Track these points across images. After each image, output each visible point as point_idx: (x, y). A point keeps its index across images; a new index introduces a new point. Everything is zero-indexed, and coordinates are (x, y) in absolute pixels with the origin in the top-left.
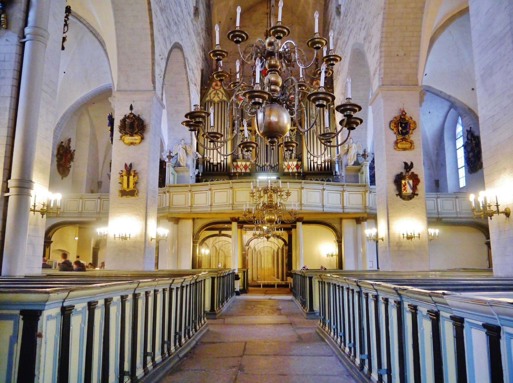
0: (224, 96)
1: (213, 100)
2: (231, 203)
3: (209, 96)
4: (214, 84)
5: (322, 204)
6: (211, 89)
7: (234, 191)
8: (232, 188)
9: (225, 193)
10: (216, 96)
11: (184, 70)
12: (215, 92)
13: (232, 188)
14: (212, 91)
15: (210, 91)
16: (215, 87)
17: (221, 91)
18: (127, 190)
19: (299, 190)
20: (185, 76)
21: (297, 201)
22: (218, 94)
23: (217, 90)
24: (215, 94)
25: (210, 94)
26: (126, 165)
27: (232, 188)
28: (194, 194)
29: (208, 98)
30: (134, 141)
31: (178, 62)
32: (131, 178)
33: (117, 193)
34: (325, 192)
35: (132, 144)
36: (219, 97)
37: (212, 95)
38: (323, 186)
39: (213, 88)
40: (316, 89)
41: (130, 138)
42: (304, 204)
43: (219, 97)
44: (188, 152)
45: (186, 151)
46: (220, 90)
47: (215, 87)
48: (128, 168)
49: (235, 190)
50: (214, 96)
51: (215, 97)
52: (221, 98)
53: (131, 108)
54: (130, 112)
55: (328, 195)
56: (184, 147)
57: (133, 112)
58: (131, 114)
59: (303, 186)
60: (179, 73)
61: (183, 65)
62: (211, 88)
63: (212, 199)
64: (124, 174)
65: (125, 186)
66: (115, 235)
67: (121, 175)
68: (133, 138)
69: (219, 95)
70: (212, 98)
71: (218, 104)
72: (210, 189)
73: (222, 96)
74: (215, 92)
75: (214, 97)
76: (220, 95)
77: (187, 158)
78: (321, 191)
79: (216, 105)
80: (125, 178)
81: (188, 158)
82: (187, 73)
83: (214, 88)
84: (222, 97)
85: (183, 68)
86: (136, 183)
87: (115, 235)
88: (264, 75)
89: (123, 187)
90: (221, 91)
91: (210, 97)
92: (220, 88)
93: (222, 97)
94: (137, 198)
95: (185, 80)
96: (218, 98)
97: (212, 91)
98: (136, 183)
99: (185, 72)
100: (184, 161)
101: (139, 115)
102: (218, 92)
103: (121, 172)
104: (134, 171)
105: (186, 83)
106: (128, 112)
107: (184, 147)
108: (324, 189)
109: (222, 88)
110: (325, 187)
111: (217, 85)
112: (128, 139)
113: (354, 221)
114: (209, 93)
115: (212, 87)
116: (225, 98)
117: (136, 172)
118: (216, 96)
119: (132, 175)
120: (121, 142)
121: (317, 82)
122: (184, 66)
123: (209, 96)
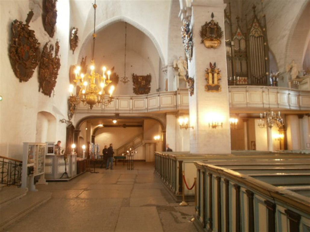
18: (213, 86)
19: (276, 94)
26: (211, 64)
30: (213, 45)
32: (216, 75)
33: (203, 88)
35: (212, 47)
40: (255, 28)
41: (210, 42)
48: (213, 66)
53: (213, 16)
54: (211, 19)
57: (214, 19)
58: (212, 21)
64: (209, 71)
65: (211, 82)
66: (209, 124)
67: (207, 72)
68: (213, 42)
80: (210, 75)
86: (219, 80)
87: (209, 124)
89: (208, 83)
94: (220, 93)
98: (219, 80)
101: (218, 23)
103: (207, 70)
104: (218, 69)
106: (209, 20)
112: (208, 43)
113: (296, 118)
117: (219, 70)
119: (216, 73)
120: (202, 45)
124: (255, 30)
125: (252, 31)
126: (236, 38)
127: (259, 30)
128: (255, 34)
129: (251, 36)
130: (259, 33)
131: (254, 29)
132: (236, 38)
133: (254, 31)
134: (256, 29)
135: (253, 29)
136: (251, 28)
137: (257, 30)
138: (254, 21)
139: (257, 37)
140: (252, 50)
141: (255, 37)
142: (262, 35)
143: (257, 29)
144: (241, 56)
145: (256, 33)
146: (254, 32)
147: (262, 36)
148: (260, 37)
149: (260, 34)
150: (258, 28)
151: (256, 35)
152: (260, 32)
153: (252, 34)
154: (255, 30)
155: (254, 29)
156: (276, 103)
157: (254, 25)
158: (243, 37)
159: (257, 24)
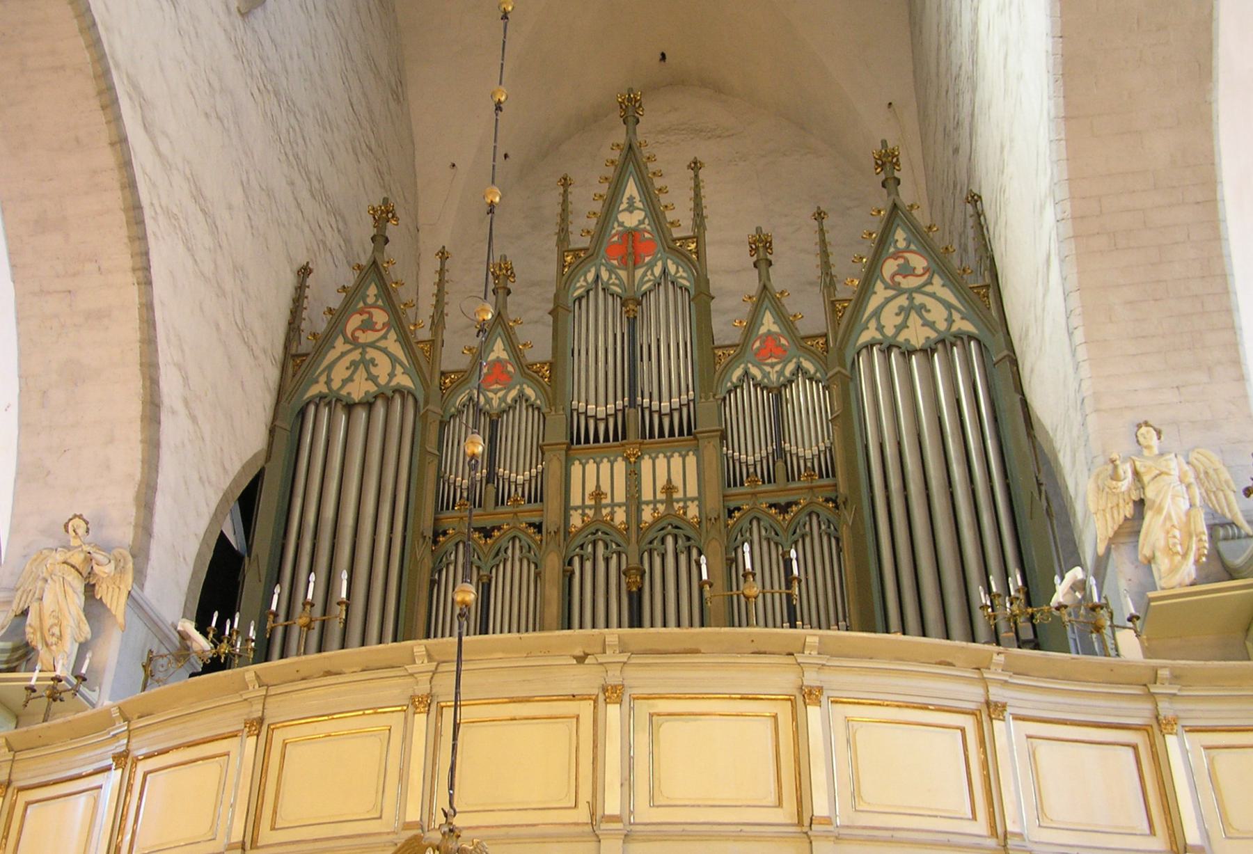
0: (399, 370)
1: (344, 392)
2: (237, 837)
3: (323, 379)
4: (355, 321)
5: (993, 827)
6: (340, 345)
7: (268, 742)
8: (261, 721)
9: (211, 770)
10: (361, 374)
11: (100, 117)
12: (356, 355)
13: (257, 725)
14: (343, 354)
15: (332, 355)
16: (358, 334)
17: (384, 351)
20: (107, 158)
21: (772, 799)
22: (369, 364)
23: (364, 346)
24: (354, 365)
25: (330, 367)
27: (261, 721)
28: (28, 804)
29: (319, 388)
31: (63, 68)
34: (1006, 733)
36: (372, 378)
37: (339, 373)
38: (985, 682)
39: (346, 341)
40: (901, 291)
42: (828, 821)
43: (372, 378)
44: (101, 592)
45: (90, 589)
46: (382, 344)
47: (358, 334)
49: (278, 737)
50: (350, 372)
51: (356, 377)
52: (383, 380)
55: (1033, 755)
56: (77, 559)
59: (811, 678)
60: (77, 140)
61: (90, 87)
62: (340, 340)
63: (121, 829)
69: (373, 370)
70: (336, 385)
71: (369, 405)
72: (121, 758)
73: (389, 370)
74: (356, 355)
75: (350, 379)
76: (383, 368)
77: (86, 628)
78: (968, 722)
79: (361, 415)
81: (96, 633)
82: (120, 142)
83: (354, 342)
84: (392, 375)
85: (95, 104)
88: (615, 262)
90: (384, 351)
91: (328, 382)
92: (384, 337)
93: (392, 375)
95: (112, 179)
96: (370, 382)
97: (343, 354)
99: (104, 135)
100: (60, 637)
102: (371, 353)
105: (114, 199)
107: (77, 559)
108: (993, 709)
109: (392, 336)
110: (997, 694)
111: (367, 326)
114: (326, 363)
115: (345, 336)
116: (404, 380)
118: (361, 374)
121: (901, 261)
122: (100, 93)
123: (323, 379)
124: (903, 301)
125: (877, 313)
126: (746, 373)
127: (933, 295)
128: (903, 326)
129: (869, 346)
130: (938, 314)
131: (888, 300)
132: (746, 373)
133: (893, 307)
134: (910, 292)
135: (880, 293)
136: (865, 290)
137: (919, 299)
138: (884, 240)
139: (927, 352)
140: (890, 450)
141: (907, 353)
142: (963, 325)
143: (919, 290)
144: (784, 508)
145: (914, 319)
146: (890, 320)
147: (963, 338)
148: (945, 342)
149: (950, 321)
150: (929, 282)
151: (917, 335)
152: (949, 306)
153: (880, 328)
154: (903, 301)
155: (888, 300)
156: (787, 814)
157: (890, 267)
158: (808, 365)
159: (919, 262)
